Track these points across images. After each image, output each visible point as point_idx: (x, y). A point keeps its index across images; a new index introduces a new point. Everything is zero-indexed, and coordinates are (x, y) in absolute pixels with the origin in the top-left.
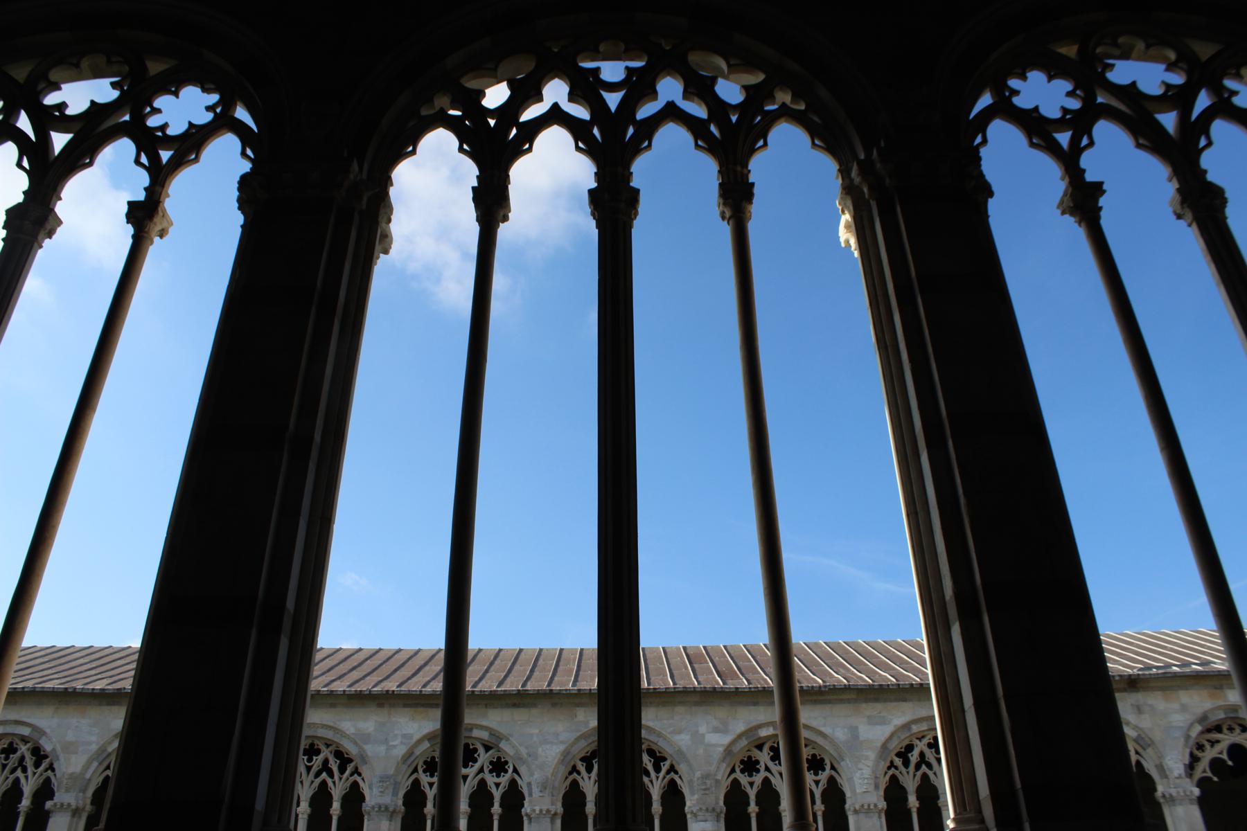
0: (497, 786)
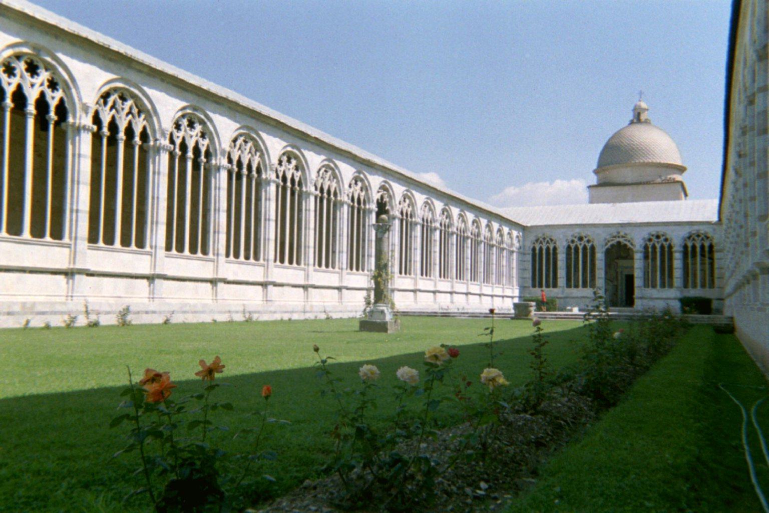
0: (589, 246)
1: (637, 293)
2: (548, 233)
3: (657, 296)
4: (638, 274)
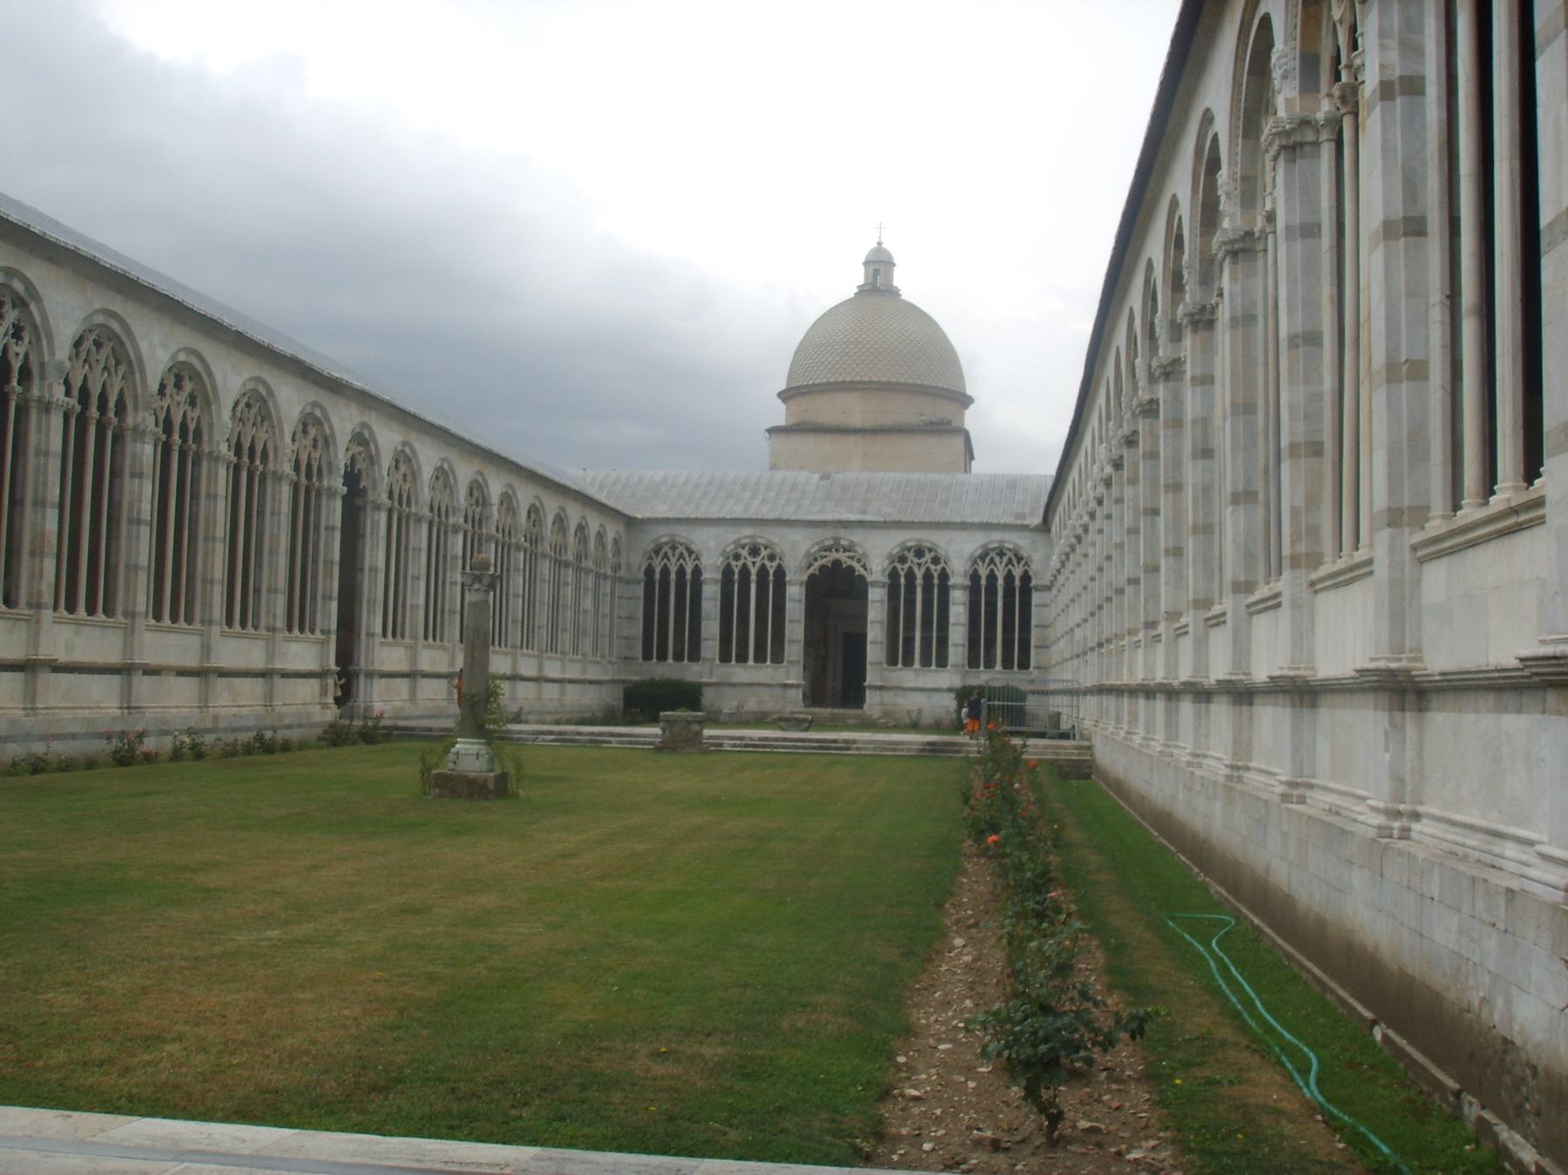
0: (771, 567)
1: (871, 677)
2: (682, 533)
3: (911, 685)
4: (875, 634)
